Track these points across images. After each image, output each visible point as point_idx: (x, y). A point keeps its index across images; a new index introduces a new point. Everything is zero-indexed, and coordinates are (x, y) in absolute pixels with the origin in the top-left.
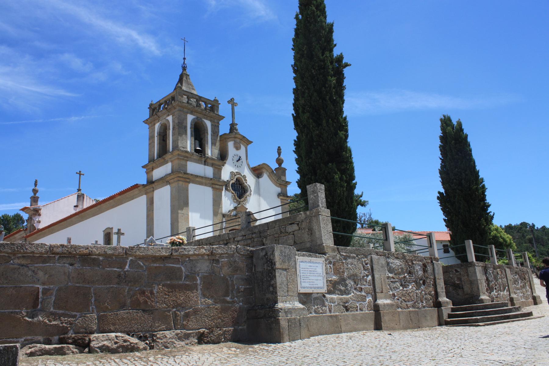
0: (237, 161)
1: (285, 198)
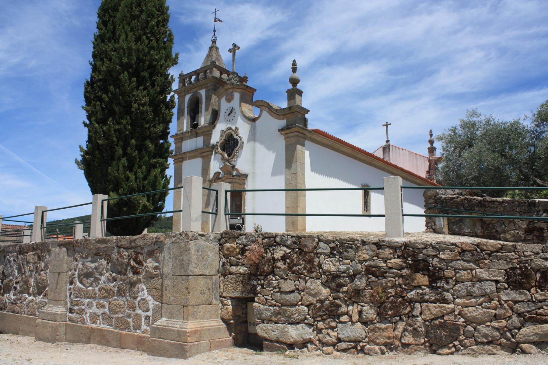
0: (229, 114)
1: (288, 131)
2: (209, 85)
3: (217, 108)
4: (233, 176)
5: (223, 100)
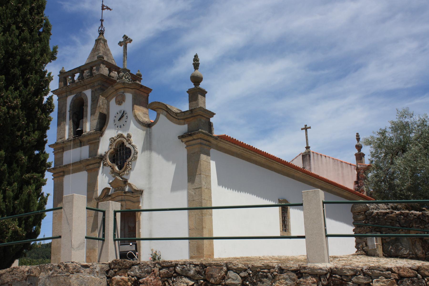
0: (120, 119)
1: (190, 138)
2: (96, 84)
3: (105, 112)
4: (125, 193)
5: (113, 102)
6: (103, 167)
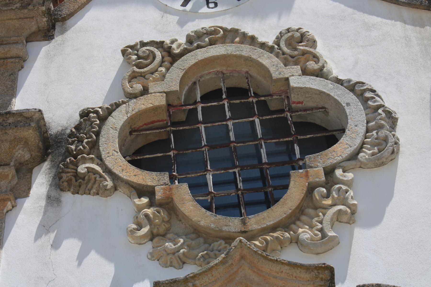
6: (52, 201)
